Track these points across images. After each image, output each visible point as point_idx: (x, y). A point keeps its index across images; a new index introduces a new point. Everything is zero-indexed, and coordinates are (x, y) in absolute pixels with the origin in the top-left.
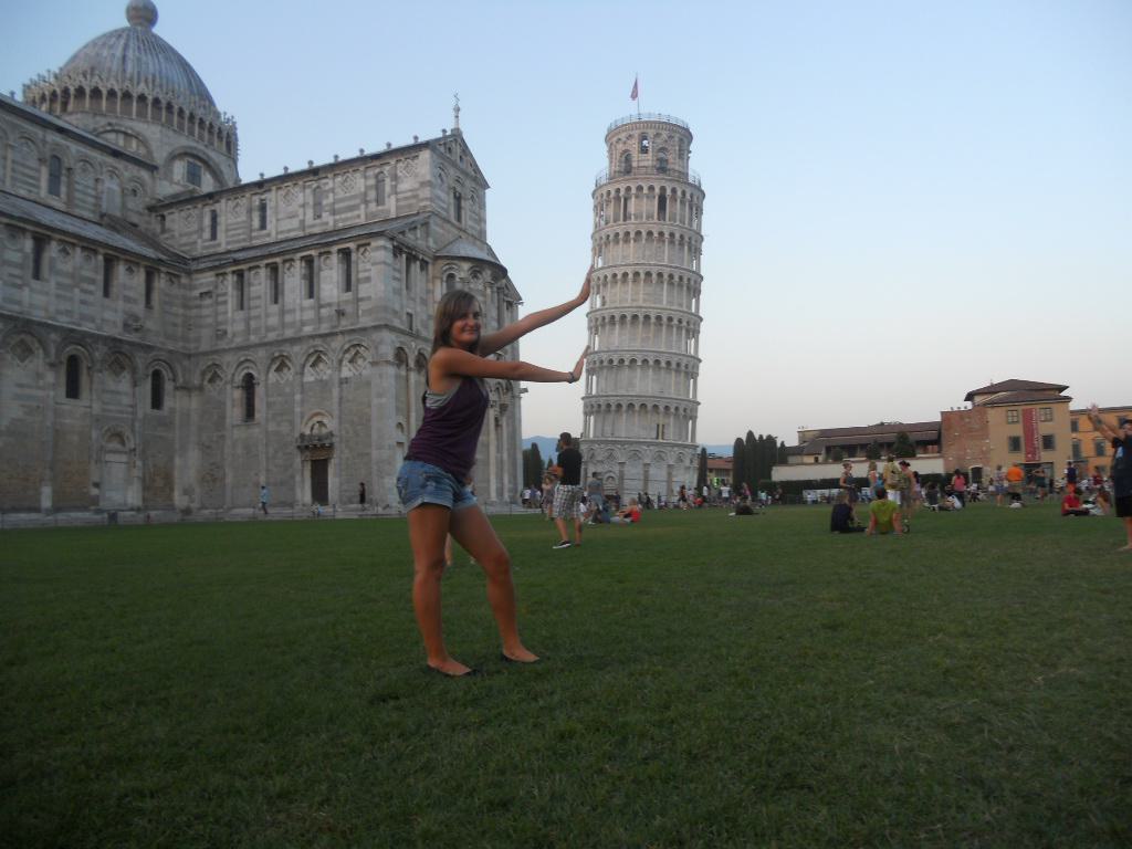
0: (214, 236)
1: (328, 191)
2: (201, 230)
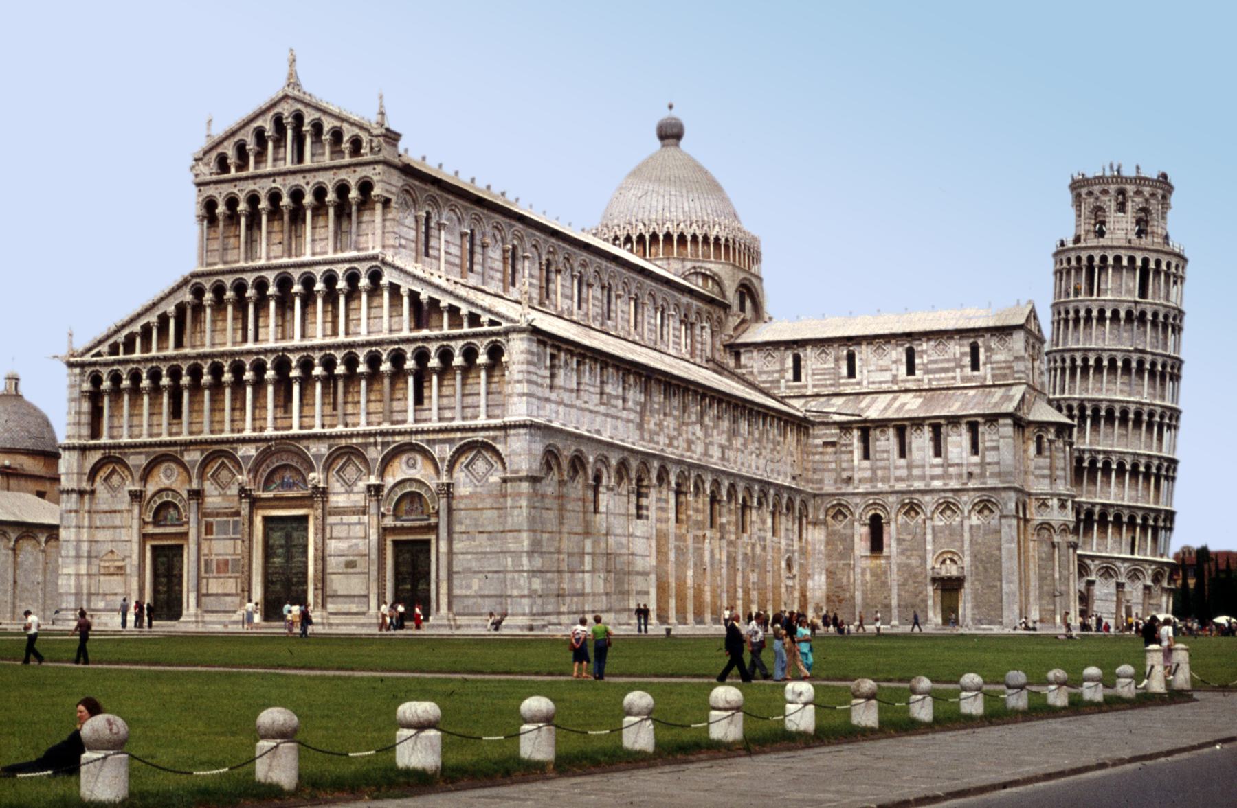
0: (797, 377)
1: (923, 352)
2: (783, 371)
